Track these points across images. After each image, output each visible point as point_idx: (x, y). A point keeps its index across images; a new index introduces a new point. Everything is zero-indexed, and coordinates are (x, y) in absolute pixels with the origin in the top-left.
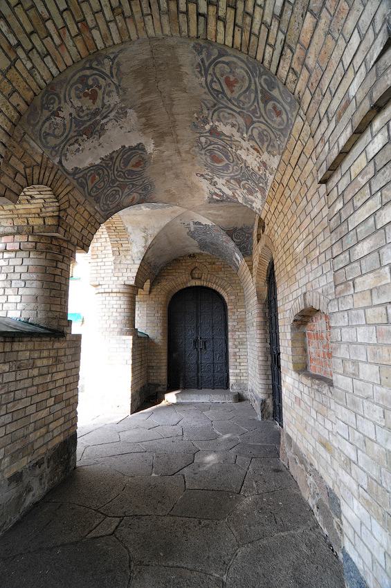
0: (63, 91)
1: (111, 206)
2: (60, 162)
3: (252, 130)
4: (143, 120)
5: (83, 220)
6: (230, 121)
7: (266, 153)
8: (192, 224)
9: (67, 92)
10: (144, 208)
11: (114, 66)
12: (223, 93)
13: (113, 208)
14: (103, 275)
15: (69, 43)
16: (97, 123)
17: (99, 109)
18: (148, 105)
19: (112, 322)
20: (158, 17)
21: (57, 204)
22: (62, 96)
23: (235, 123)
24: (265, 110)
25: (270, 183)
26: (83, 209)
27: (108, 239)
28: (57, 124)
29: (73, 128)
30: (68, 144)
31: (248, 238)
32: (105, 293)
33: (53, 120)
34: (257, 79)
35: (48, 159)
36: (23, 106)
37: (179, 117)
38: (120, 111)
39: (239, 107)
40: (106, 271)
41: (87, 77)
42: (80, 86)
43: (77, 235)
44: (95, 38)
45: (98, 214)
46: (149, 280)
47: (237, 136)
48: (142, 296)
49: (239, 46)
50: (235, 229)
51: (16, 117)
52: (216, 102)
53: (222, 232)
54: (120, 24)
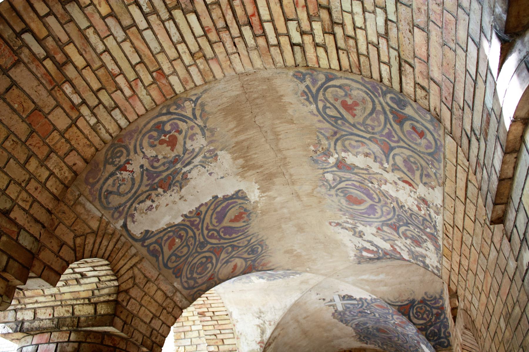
0: (133, 142)
1: (200, 281)
2: (125, 226)
3: (394, 158)
4: (241, 161)
5: (154, 304)
6: (360, 150)
7: (421, 185)
8: (337, 299)
9: (138, 143)
10: (255, 280)
11: (198, 107)
12: (343, 118)
13: (203, 283)
15: (142, 92)
16: (177, 172)
17: (179, 156)
18: (245, 144)
20: (246, 53)
21: (116, 283)
22: (131, 147)
23: (368, 151)
24: (403, 132)
25: (440, 227)
26: (155, 288)
28: (124, 180)
29: (145, 181)
30: (137, 201)
31: (438, 315)
33: (119, 175)
34: (381, 99)
35: (108, 223)
36: (80, 164)
37: (290, 153)
38: (208, 155)
39: (369, 133)
41: (164, 123)
42: (155, 134)
43: (143, 328)
44: (173, 84)
45: (178, 294)
47: (375, 168)
49: (348, 68)
50: (412, 303)
51: (70, 178)
52: (336, 129)
53: (391, 310)
54: (201, 67)
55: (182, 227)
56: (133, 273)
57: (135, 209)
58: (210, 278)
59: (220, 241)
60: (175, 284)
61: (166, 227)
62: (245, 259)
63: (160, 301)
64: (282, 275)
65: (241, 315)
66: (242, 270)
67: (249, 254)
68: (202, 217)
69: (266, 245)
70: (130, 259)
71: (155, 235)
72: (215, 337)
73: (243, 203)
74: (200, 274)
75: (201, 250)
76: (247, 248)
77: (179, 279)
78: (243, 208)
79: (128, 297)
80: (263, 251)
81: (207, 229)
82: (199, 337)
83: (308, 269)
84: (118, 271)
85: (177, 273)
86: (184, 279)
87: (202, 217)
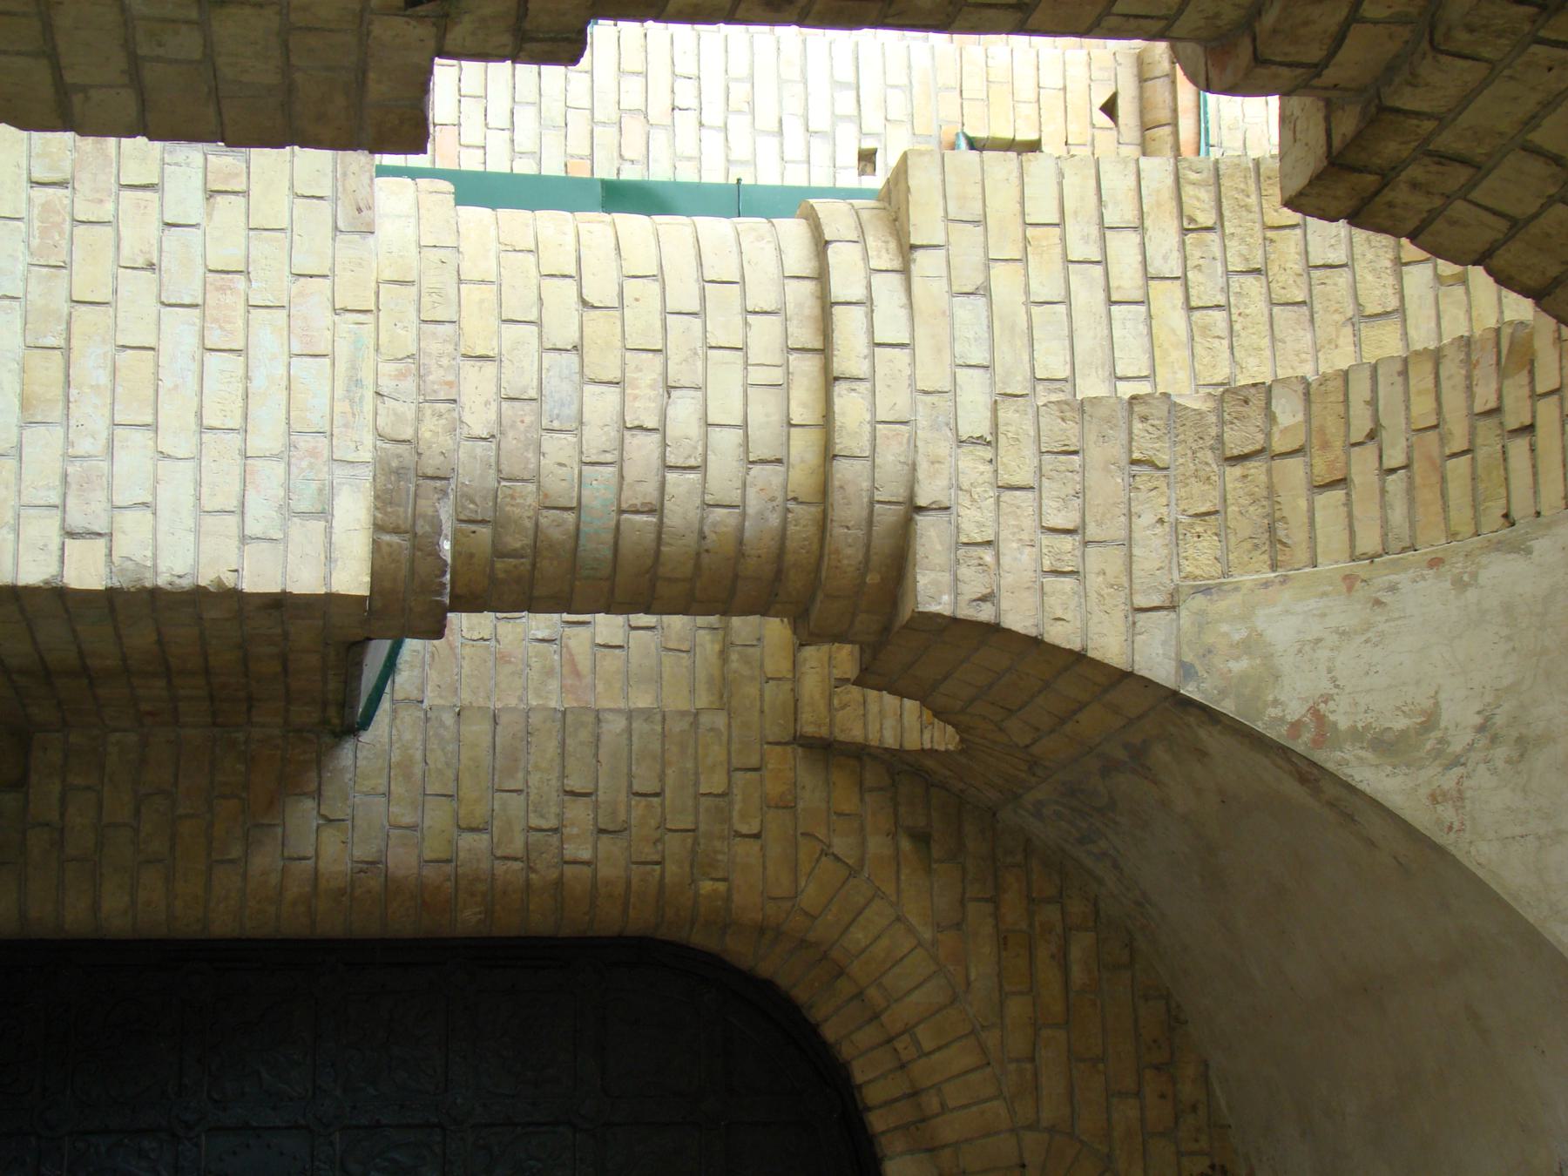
14: (1005, 281)
19: (521, 375)
27: (1385, 343)
32: (826, 306)
40: (1049, 322)
46: (943, 738)
48: (777, 663)
65: (1508, 609)
72: (1358, 434)
82: (1362, 317)
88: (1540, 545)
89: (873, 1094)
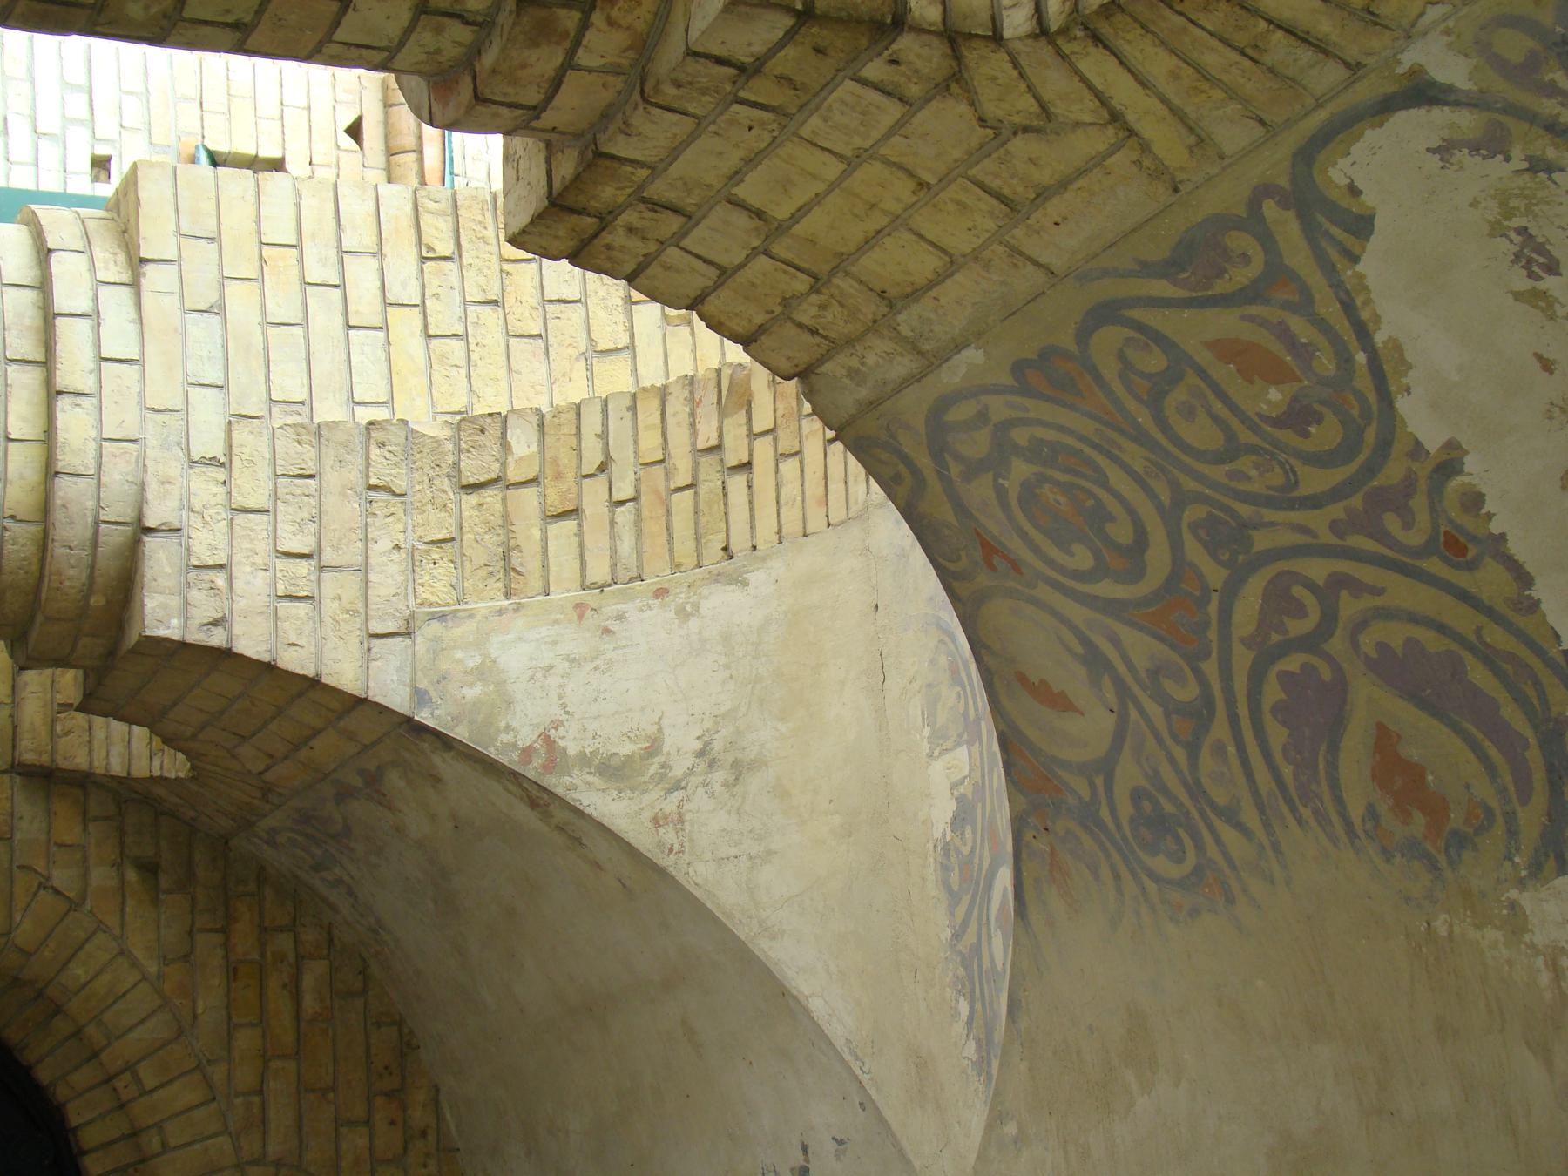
1: (980, 491)
2: (1422, 92)
5: (856, 233)
10: (947, 771)
13: (961, 508)
14: (240, 300)
26: (962, 243)
27: (615, 378)
32: (48, 317)
43: (705, 162)
45: (904, 365)
46: (173, 765)
55: (1370, 435)
56: (1077, 124)
57: (1537, 166)
58: (990, 550)
59: (1247, 642)
60: (972, 356)
61: (1379, 338)
62: (1106, 767)
63: (869, 263)
64: (976, 950)
65: (726, 638)
66: (1032, 733)
67: (1137, 796)
68: (1434, 566)
69: (1195, 912)
70: (1177, 113)
71: (1329, 270)
72: (589, 466)
73: (1512, 833)
74: (1029, 493)
75: (1194, 527)
76: (1184, 797)
77: (1007, 380)
78: (1478, 831)
79: (914, 90)
80: (1151, 886)
81: (1339, 582)
82: (595, 352)
83: (1011, 1129)
84: (1097, 39)
85: (1042, 373)
86: (999, 408)
87: (1434, 566)
88: (755, 578)
89: (89, 1137)
